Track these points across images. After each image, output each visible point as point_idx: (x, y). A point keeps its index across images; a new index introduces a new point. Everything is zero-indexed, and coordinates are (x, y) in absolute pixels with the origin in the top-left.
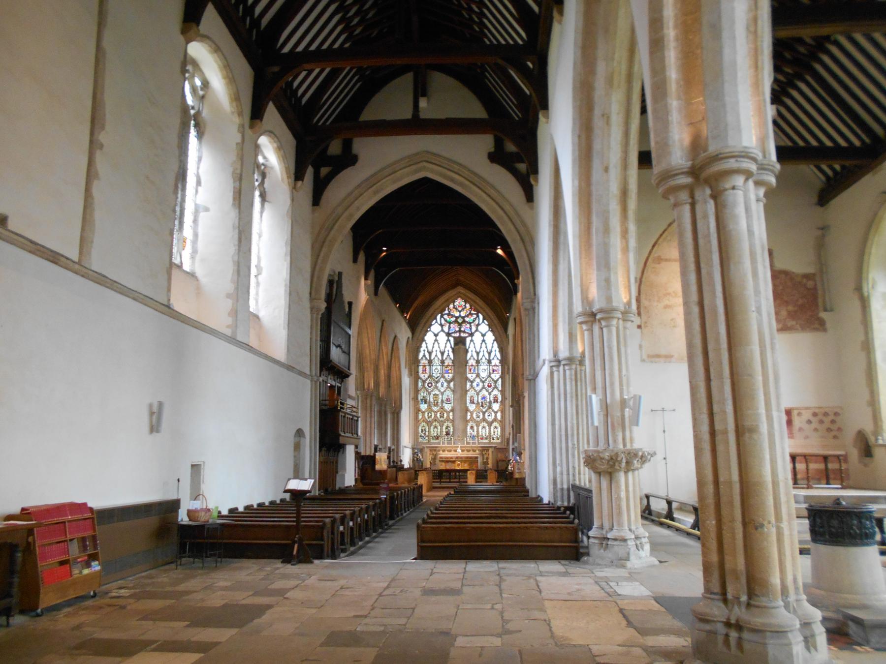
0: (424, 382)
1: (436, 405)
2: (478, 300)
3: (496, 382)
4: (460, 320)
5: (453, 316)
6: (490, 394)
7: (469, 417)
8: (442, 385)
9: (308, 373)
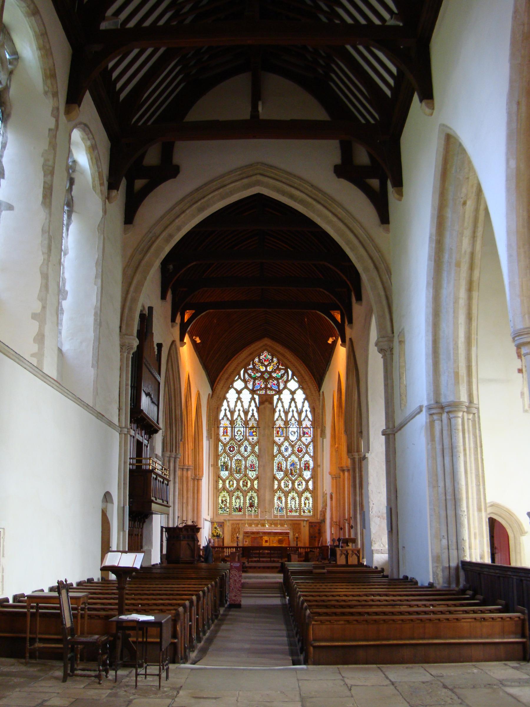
0: (225, 445)
1: (239, 472)
2: (288, 354)
3: (307, 446)
4: (266, 376)
5: (258, 371)
6: (300, 460)
7: (276, 487)
8: (246, 449)
9: (117, 424)
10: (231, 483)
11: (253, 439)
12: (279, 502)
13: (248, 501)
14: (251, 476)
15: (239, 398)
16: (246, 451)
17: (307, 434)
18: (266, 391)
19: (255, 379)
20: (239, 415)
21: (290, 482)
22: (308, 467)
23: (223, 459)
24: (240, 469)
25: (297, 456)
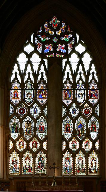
0: (15, 107)
1: (28, 133)
4: (55, 40)
5: (48, 35)
6: (87, 121)
7: (64, 147)
10: (21, 144)
11: (42, 101)
12: (67, 163)
13: (37, 162)
14: (40, 138)
15: (29, 62)
16: (35, 113)
17: (94, 96)
18: (55, 55)
19: (44, 43)
20: (29, 78)
21: (78, 143)
22: (95, 128)
23: (13, 122)
24: (30, 131)
25: (84, 117)
